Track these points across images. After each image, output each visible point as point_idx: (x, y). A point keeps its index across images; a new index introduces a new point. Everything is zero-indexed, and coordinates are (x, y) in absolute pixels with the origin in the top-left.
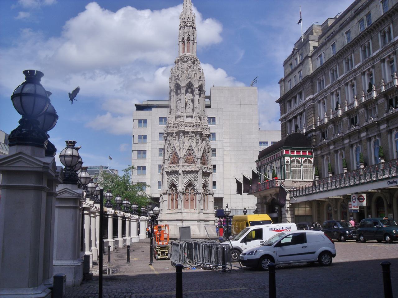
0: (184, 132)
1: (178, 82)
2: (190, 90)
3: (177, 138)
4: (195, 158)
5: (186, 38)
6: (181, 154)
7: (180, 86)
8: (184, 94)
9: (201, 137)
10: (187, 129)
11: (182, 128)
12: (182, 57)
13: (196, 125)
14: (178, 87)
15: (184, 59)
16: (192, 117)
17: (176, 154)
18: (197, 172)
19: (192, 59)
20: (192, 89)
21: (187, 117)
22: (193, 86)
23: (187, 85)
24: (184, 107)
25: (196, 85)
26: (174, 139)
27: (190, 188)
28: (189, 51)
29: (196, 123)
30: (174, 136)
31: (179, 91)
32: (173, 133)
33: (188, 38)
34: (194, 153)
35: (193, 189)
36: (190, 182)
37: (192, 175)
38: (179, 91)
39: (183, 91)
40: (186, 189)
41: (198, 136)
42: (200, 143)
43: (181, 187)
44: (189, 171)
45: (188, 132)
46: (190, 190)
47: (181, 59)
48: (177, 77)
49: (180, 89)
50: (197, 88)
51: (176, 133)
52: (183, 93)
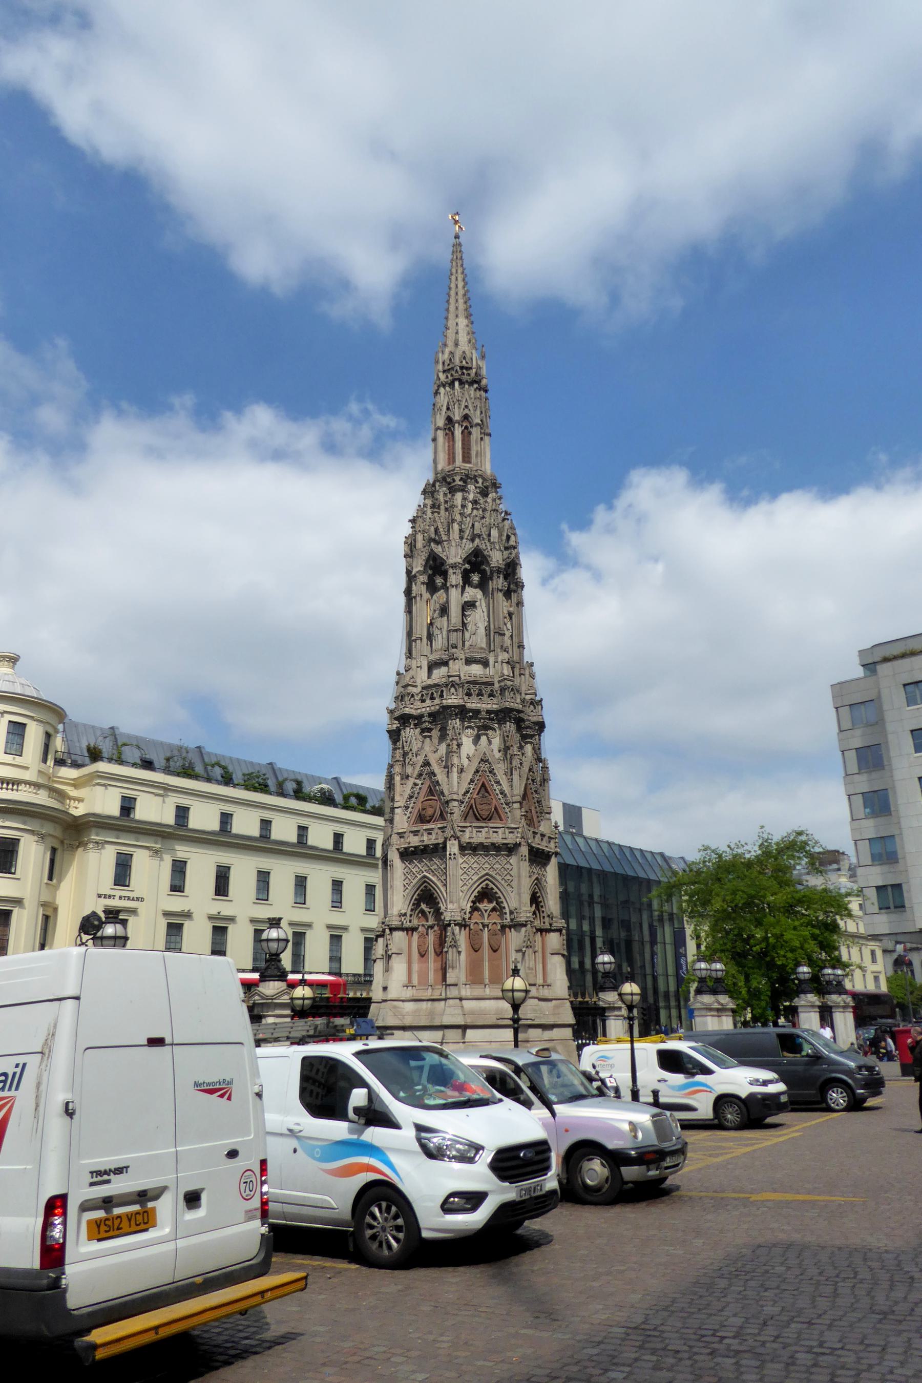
0: (462, 712)
1: (438, 549)
2: (475, 578)
3: (435, 733)
4: (502, 801)
5: (457, 417)
6: (455, 785)
7: (443, 562)
8: (460, 590)
9: (519, 729)
10: (473, 704)
11: (453, 699)
12: (449, 476)
13: (503, 690)
14: (436, 567)
15: (454, 481)
16: (486, 664)
17: (434, 790)
18: (511, 849)
19: (480, 480)
20: (483, 573)
21: (469, 661)
22: (488, 564)
23: (467, 560)
24: (456, 631)
25: (497, 558)
26: (425, 737)
27: (485, 906)
28: (469, 457)
29: (499, 682)
30: (424, 726)
31: (439, 581)
32: (421, 716)
33: (466, 417)
34: (498, 783)
35: (499, 909)
36: (487, 885)
37: (493, 861)
38: (439, 581)
39: (455, 578)
40: (474, 909)
41: (510, 727)
42: (515, 750)
43: (456, 902)
44: (481, 844)
45: (477, 712)
46: (486, 915)
47: (444, 479)
48: (433, 536)
49: (444, 574)
50: (499, 571)
51: (430, 715)
52: (454, 583)
